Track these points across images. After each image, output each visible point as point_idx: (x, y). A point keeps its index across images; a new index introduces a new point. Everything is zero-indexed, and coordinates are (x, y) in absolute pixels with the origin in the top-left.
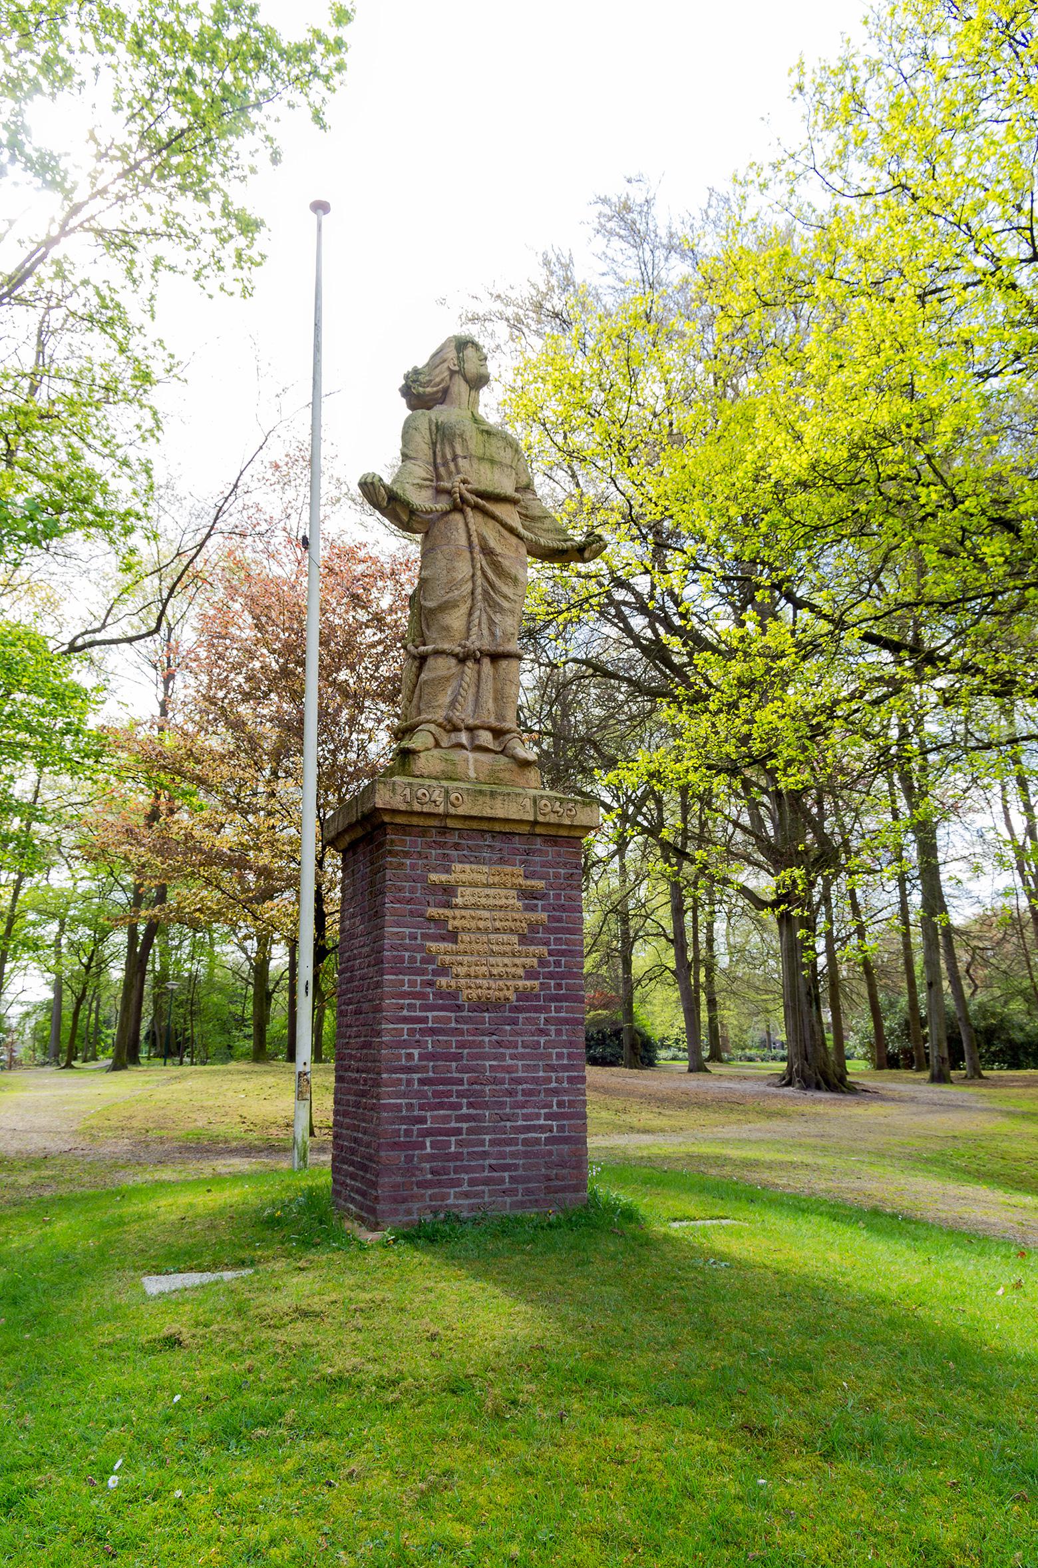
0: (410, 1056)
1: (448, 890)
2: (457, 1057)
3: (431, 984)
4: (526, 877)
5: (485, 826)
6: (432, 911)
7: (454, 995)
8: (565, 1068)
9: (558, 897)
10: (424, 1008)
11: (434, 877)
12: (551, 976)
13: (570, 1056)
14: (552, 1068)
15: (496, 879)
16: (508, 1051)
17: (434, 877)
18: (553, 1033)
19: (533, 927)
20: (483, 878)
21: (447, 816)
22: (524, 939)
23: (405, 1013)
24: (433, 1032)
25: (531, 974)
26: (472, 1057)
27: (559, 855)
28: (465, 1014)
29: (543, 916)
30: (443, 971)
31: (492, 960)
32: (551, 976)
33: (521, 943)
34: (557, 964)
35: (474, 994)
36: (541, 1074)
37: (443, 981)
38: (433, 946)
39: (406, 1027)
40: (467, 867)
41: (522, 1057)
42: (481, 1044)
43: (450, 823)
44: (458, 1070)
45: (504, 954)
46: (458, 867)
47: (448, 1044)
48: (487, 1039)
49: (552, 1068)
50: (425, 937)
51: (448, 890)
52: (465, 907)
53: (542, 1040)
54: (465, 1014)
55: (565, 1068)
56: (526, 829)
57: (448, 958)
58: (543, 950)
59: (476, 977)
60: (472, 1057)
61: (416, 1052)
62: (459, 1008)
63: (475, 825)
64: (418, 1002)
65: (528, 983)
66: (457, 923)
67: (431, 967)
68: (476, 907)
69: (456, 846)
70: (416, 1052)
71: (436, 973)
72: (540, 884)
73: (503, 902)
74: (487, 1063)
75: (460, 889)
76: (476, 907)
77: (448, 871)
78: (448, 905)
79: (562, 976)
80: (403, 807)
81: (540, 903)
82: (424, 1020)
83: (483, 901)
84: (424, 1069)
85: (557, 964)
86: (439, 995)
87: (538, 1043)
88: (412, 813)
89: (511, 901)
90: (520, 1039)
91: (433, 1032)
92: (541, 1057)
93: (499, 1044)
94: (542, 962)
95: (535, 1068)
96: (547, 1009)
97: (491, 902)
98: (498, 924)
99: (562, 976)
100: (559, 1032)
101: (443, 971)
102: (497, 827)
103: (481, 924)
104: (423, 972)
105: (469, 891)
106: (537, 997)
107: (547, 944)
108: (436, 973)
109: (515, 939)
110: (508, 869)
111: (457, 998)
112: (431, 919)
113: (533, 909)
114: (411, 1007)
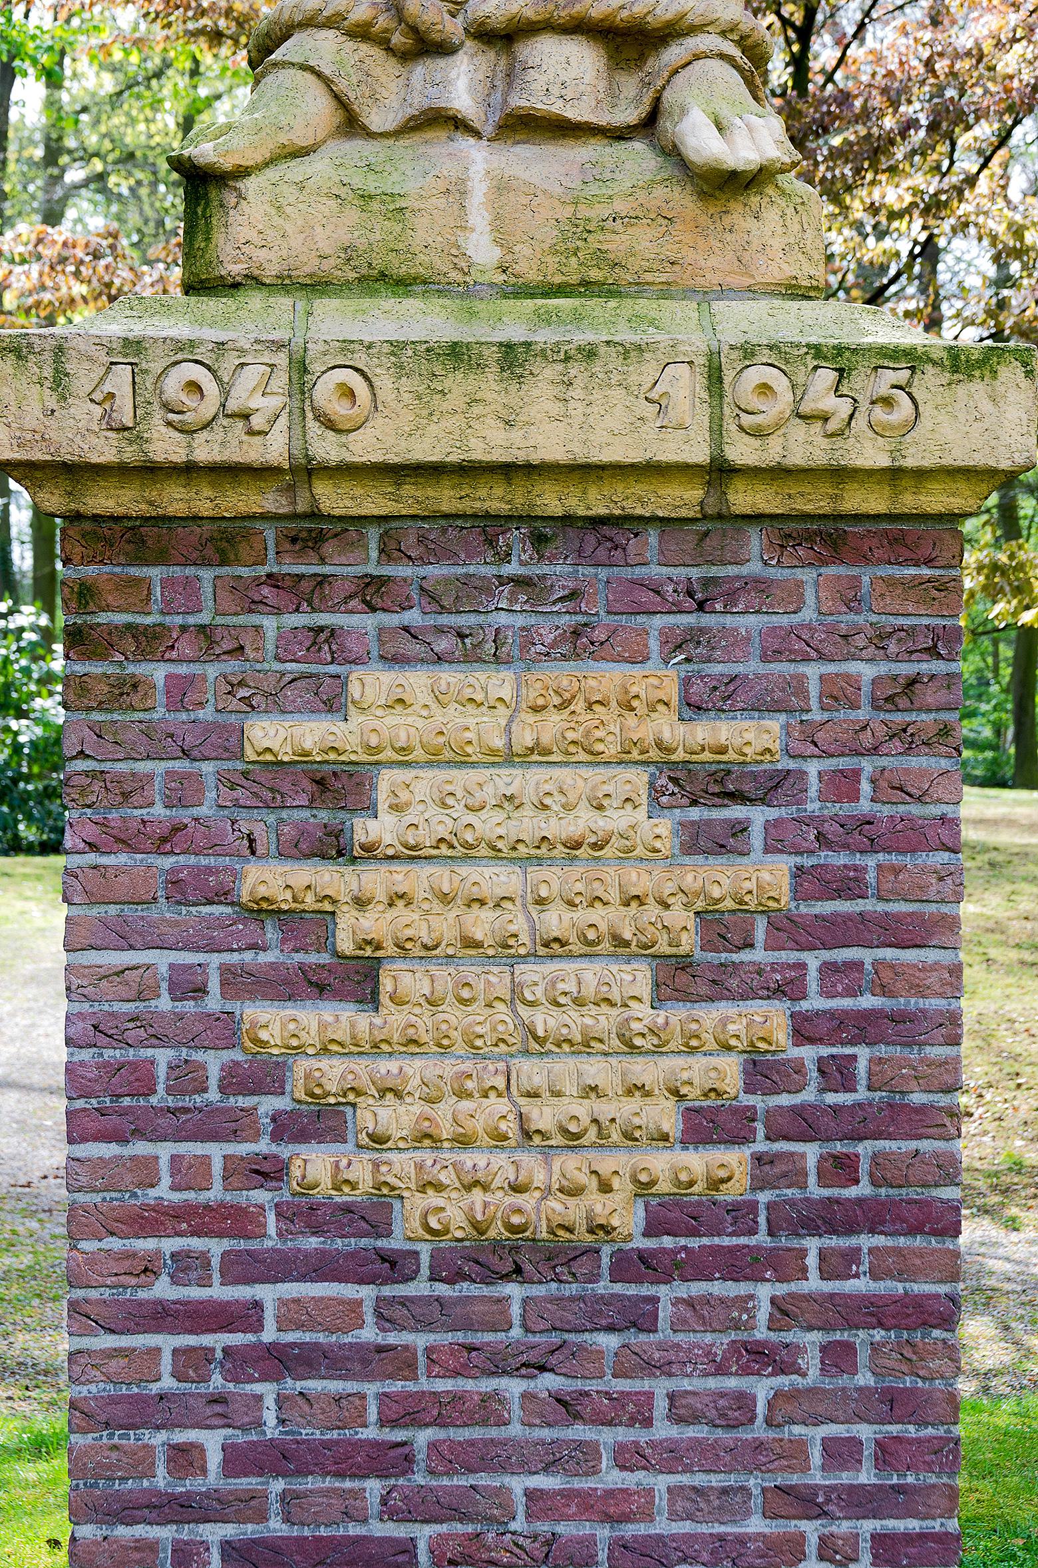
0: (185, 1458)
1: (337, 785)
2: (389, 1460)
3: (268, 1172)
4: (693, 707)
5: (493, 498)
6: (267, 879)
7: (372, 1215)
8: (861, 1502)
9: (842, 785)
10: (242, 1268)
11: (269, 734)
12: (803, 1124)
13: (886, 1454)
14: (805, 1502)
15: (552, 726)
16: (607, 1437)
17: (269, 734)
18: (811, 1362)
19: (722, 926)
20: (489, 729)
21: (308, 470)
22: (677, 978)
23: (163, 1289)
24: (279, 1362)
25: (708, 1124)
26: (449, 1458)
27: (852, 602)
28: (420, 1287)
29: (767, 876)
30: (321, 1121)
31: (531, 1072)
32: (803, 1124)
33: (662, 993)
34: (837, 1074)
35: (455, 1212)
36: (756, 1525)
37: (315, 1164)
38: (272, 1022)
39: (167, 1343)
40: (417, 681)
41: (672, 1457)
42: (488, 1410)
43: (333, 498)
44: (390, 1512)
45: (586, 1045)
46: (370, 683)
47: (347, 1409)
48: (513, 1387)
49: (805, 1502)
50: (237, 982)
51: (337, 785)
52: (412, 855)
53: (762, 1388)
54: (420, 1287)
55: (861, 1502)
56: (685, 498)
57: (333, 1073)
58: (771, 1020)
59: (463, 1142)
60: (449, 1458)
61: (212, 1442)
62: (395, 1266)
63: (447, 498)
64: (216, 1247)
65: (697, 1162)
66: (374, 923)
67: (268, 1105)
68: (457, 850)
69: (372, 593)
70: (212, 1442)
71: (289, 1128)
72: (752, 737)
73: (582, 822)
74: (518, 1484)
75: (387, 780)
76: (457, 850)
77: (333, 703)
78: (335, 847)
79: (859, 1124)
80: (104, 450)
81: (758, 816)
82: (246, 1316)
83: (489, 824)
84: (250, 1507)
85: (837, 1074)
86: (306, 1214)
87: (744, 1401)
88: (151, 471)
89: (616, 820)
90: (661, 1387)
91: (279, 1362)
92: (756, 1455)
93: (568, 1407)
94: (762, 1071)
95: (730, 1501)
96: (786, 1266)
97: (528, 825)
98: (555, 921)
99: (859, 1124)
100: (838, 1357)
101: (321, 1121)
102: (551, 500)
103: (482, 924)
104: (231, 1126)
105: (425, 783)
106: (741, 1215)
107: (788, 988)
108: (289, 1128)
109: (638, 978)
110: (606, 677)
111: (381, 1228)
112: (261, 911)
113: (724, 842)
114: (186, 1266)
